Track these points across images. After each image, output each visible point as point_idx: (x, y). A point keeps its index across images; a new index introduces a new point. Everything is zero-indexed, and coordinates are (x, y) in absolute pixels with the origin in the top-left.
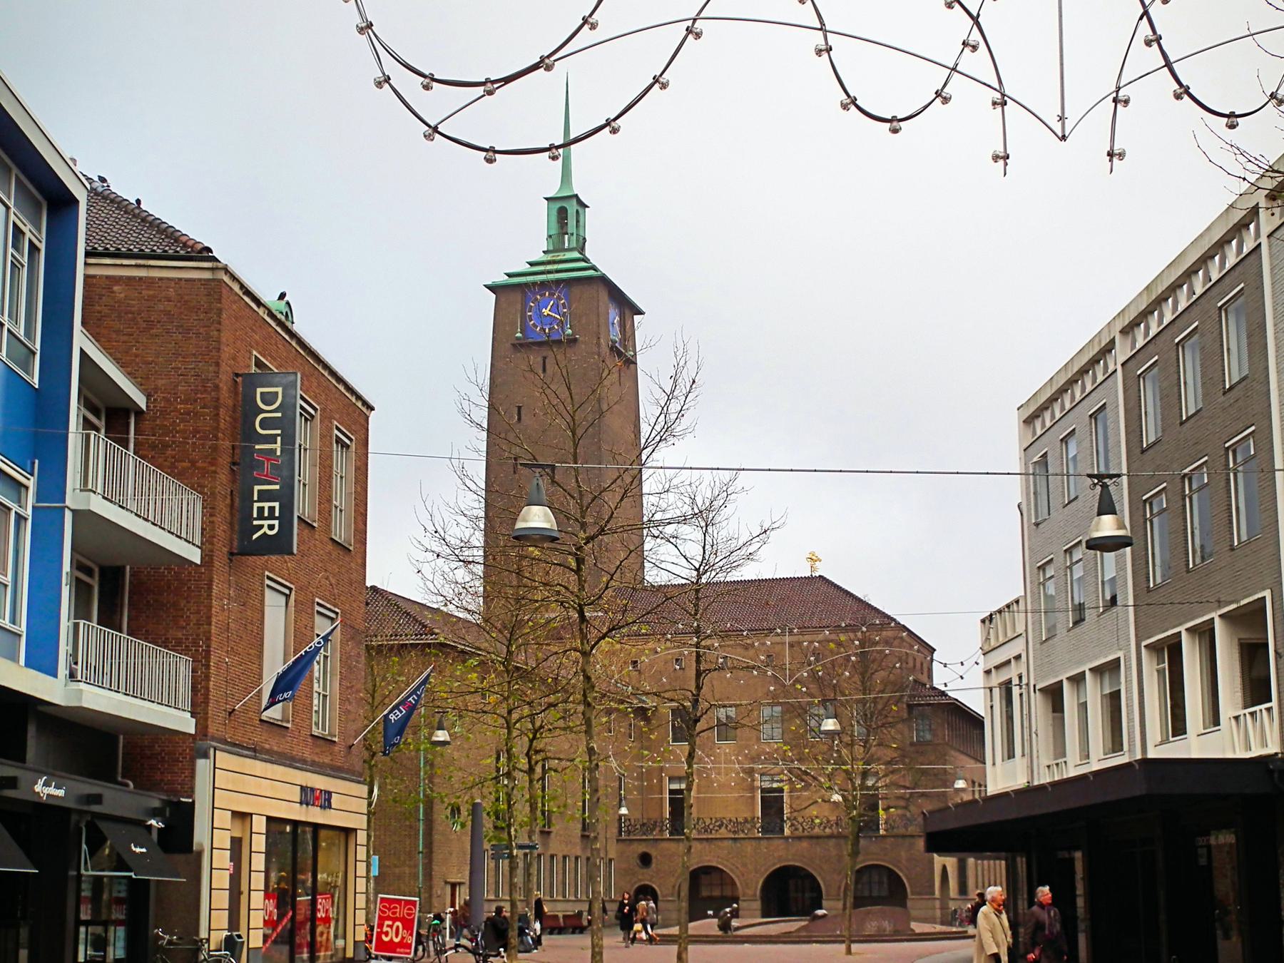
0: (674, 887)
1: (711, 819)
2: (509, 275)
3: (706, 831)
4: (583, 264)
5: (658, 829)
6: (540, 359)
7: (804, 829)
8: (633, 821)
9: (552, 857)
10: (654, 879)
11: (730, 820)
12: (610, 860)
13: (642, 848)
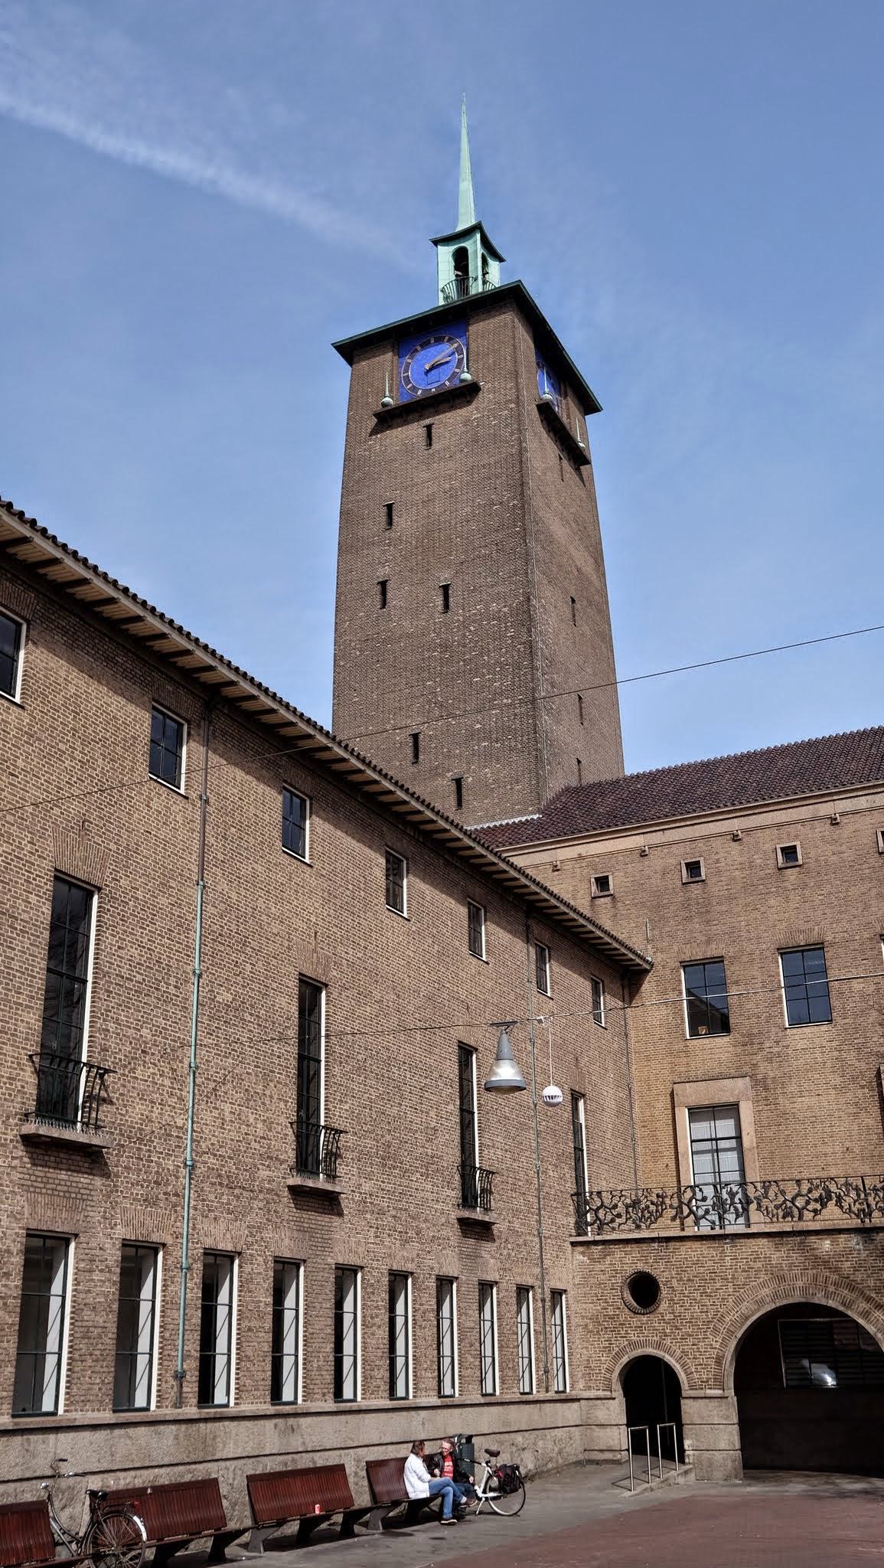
0: (719, 1361)
1: (798, 1182)
3: (788, 1214)
6: (422, 431)
9: (345, 1275)
10: (668, 1341)
11: (847, 1184)
12: (557, 1294)
13: (631, 1262)
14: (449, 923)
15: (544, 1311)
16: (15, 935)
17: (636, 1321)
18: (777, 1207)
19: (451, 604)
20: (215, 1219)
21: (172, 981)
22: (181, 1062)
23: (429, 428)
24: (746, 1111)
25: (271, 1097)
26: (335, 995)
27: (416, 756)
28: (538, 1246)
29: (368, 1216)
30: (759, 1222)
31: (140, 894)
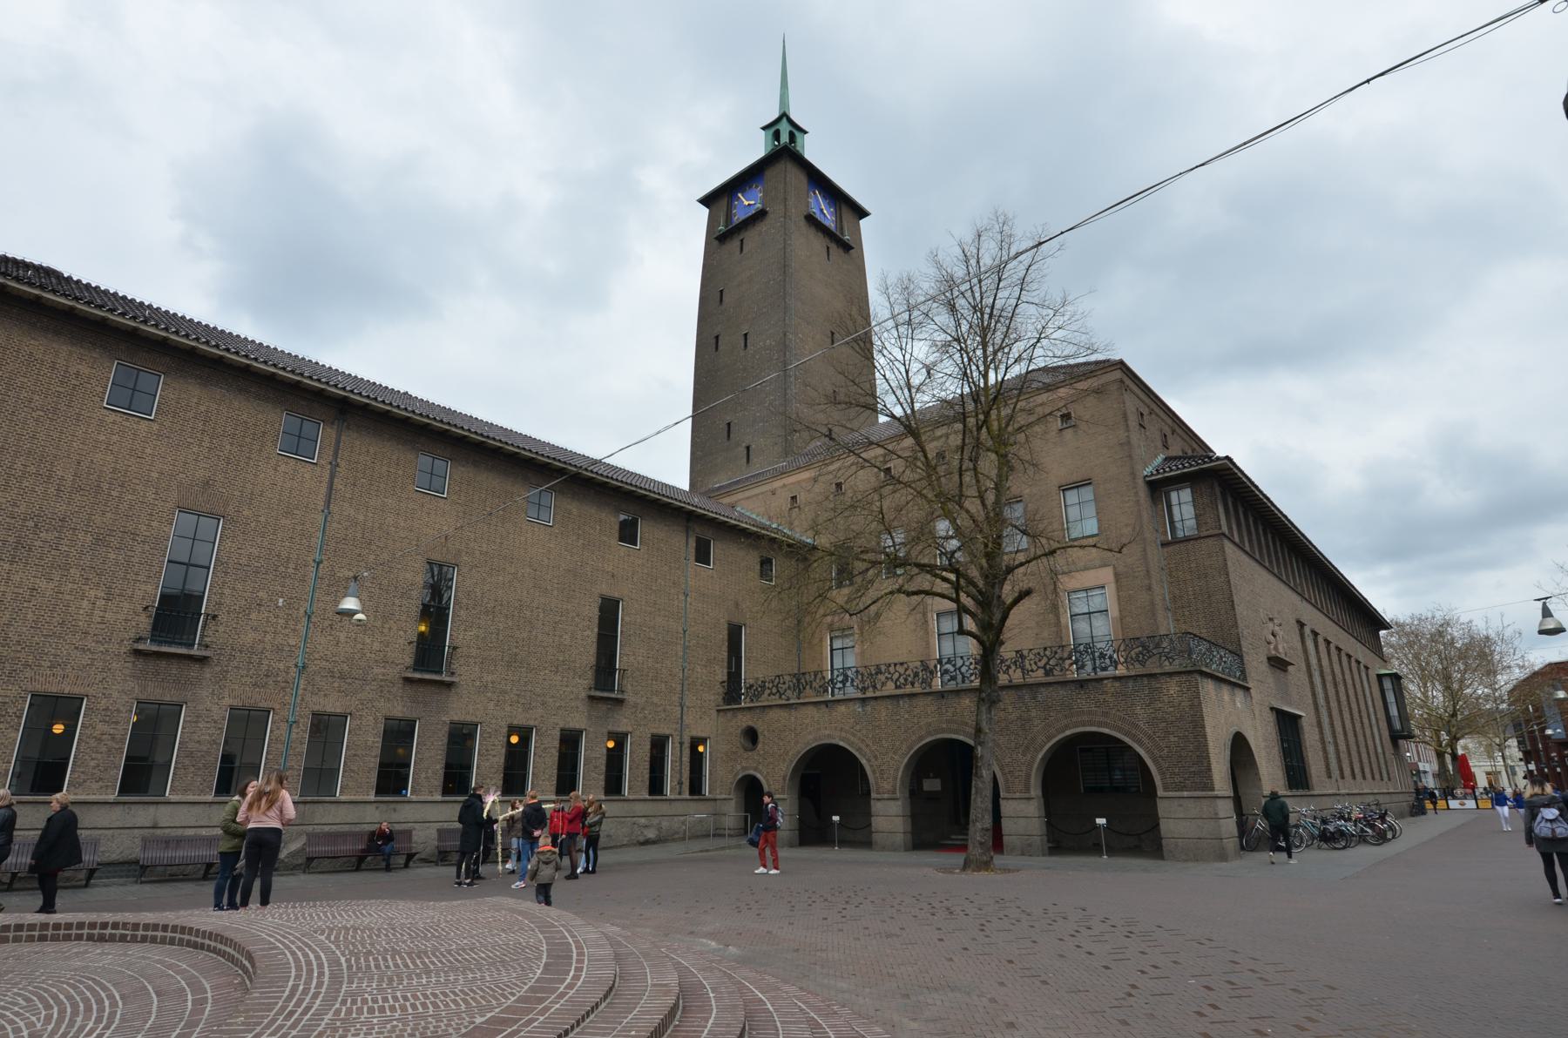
0: (784, 779)
5: (767, 692)
6: (739, 243)
7: (963, 677)
13: (745, 720)
14: (598, 527)
15: (681, 750)
16: (136, 544)
17: (745, 755)
18: (820, 687)
19: (748, 344)
20: (325, 695)
21: (291, 565)
22: (298, 609)
23: (742, 240)
25: (390, 629)
26: (465, 570)
27: (729, 436)
28: (680, 712)
29: (489, 694)
31: (262, 519)
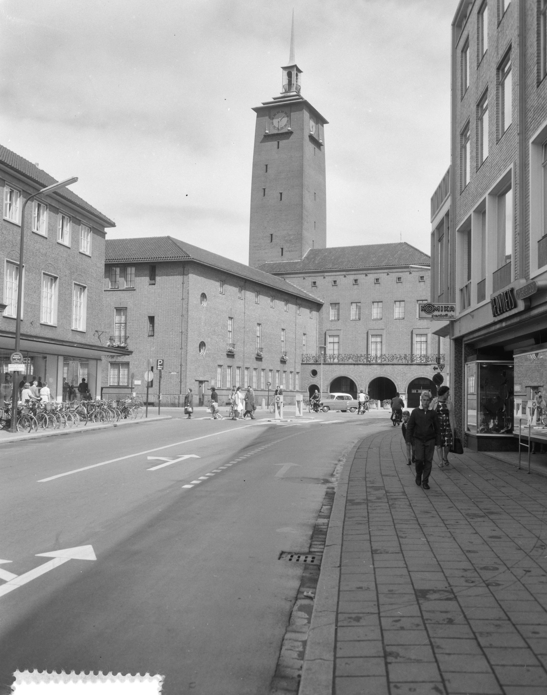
2: (264, 104)
4: (297, 97)
7: (388, 360)
8: (308, 355)
11: (354, 355)
19: (282, 199)
23: (278, 142)
24: (341, 336)
30: (336, 361)
